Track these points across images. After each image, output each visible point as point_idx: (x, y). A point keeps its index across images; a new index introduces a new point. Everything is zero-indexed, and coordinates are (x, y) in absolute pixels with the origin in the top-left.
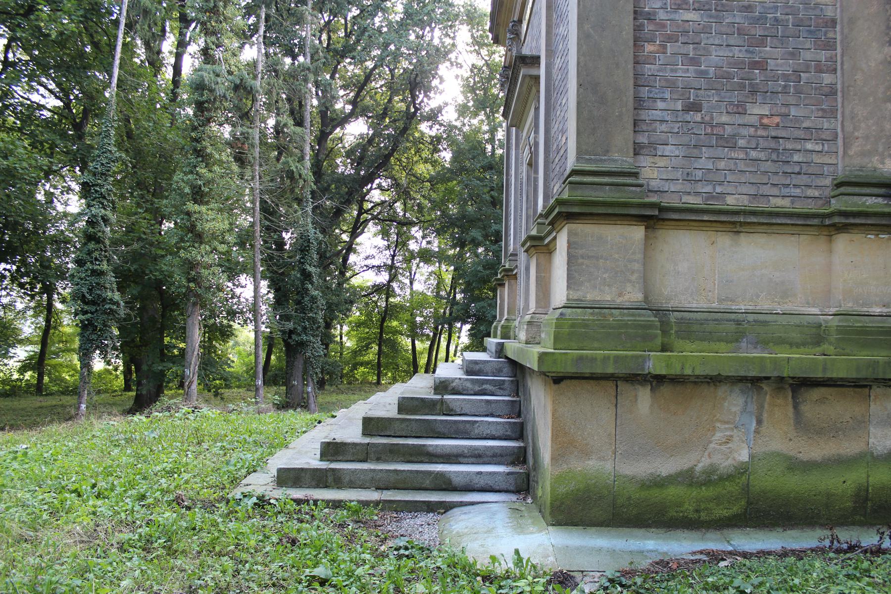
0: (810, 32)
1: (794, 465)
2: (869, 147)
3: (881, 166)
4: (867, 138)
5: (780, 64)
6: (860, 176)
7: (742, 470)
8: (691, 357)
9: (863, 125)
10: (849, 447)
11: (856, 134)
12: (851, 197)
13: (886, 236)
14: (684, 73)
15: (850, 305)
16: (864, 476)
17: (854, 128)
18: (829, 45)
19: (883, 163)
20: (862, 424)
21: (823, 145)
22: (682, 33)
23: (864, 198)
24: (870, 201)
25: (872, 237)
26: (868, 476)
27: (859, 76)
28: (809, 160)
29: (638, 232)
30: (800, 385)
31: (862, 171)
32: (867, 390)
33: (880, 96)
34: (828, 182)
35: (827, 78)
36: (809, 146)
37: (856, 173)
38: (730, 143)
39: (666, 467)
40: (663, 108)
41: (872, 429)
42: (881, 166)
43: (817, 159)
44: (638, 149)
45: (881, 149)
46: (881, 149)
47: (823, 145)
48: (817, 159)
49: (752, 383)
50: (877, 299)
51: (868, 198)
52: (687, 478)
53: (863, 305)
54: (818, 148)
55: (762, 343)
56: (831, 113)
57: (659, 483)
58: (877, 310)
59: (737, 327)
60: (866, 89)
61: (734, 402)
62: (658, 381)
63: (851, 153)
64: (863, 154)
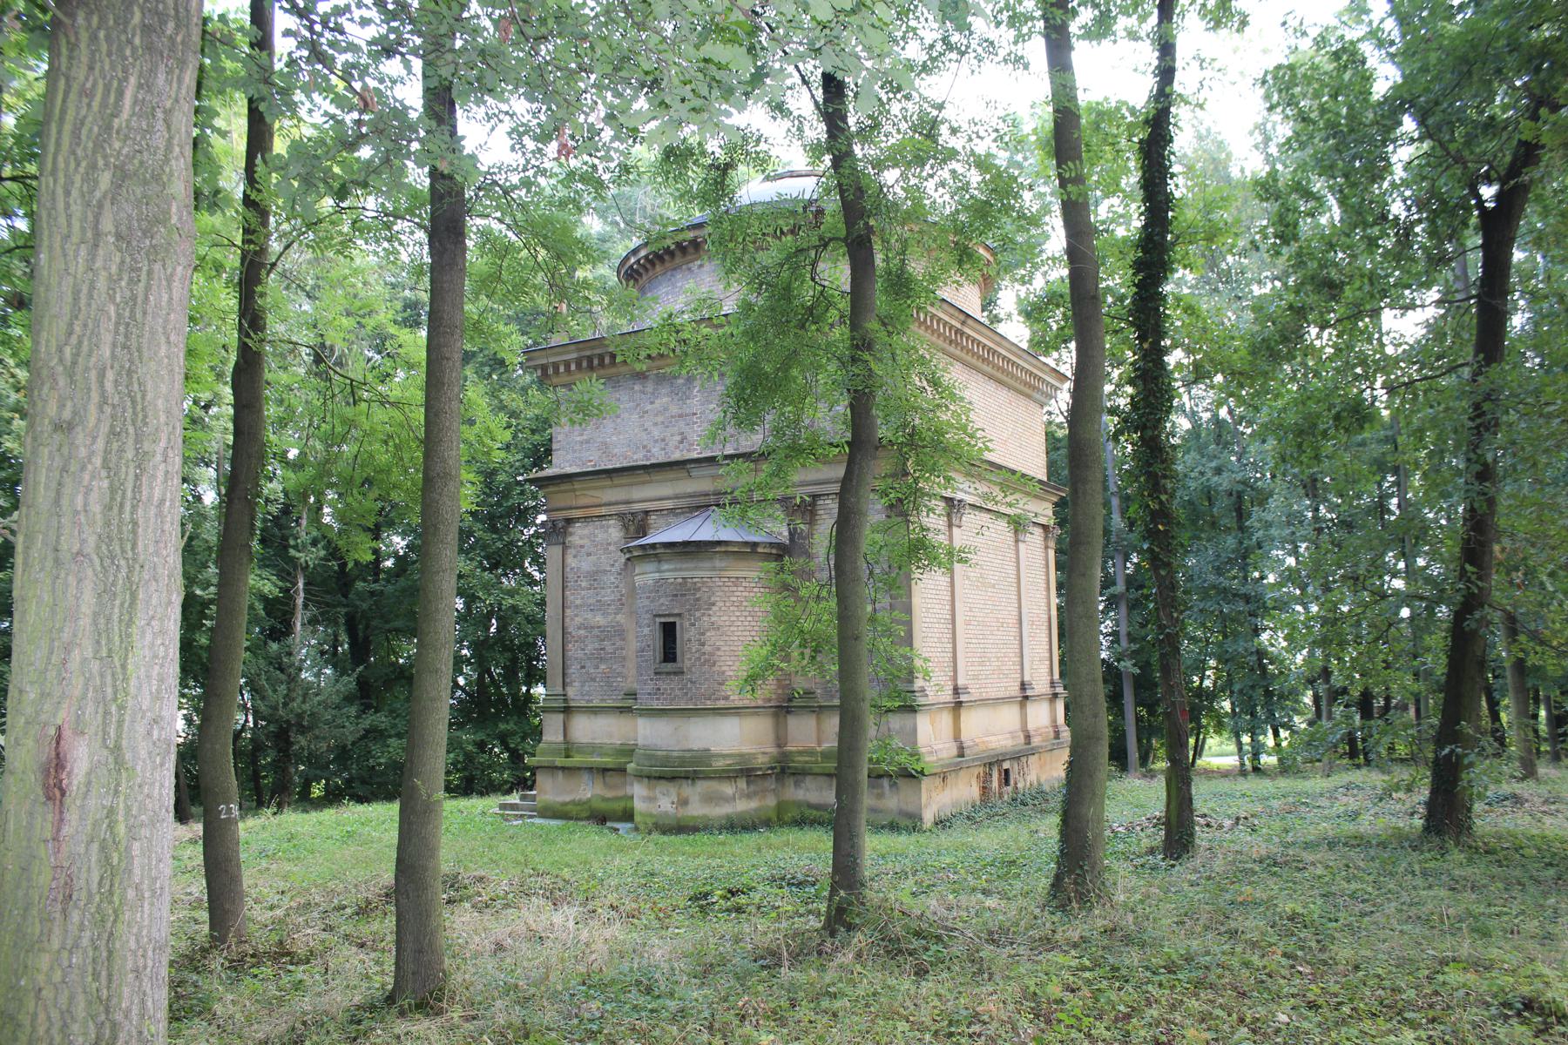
1: (604, 799)
5: (609, 649)
7: (589, 800)
8: (577, 760)
10: (620, 793)
14: (580, 654)
22: (581, 640)
29: (561, 716)
30: (604, 771)
38: (593, 680)
39: (568, 799)
40: (573, 669)
44: (564, 685)
49: (590, 769)
52: (573, 802)
55: (601, 755)
57: (566, 804)
59: (594, 749)
61: (586, 776)
62: (563, 768)
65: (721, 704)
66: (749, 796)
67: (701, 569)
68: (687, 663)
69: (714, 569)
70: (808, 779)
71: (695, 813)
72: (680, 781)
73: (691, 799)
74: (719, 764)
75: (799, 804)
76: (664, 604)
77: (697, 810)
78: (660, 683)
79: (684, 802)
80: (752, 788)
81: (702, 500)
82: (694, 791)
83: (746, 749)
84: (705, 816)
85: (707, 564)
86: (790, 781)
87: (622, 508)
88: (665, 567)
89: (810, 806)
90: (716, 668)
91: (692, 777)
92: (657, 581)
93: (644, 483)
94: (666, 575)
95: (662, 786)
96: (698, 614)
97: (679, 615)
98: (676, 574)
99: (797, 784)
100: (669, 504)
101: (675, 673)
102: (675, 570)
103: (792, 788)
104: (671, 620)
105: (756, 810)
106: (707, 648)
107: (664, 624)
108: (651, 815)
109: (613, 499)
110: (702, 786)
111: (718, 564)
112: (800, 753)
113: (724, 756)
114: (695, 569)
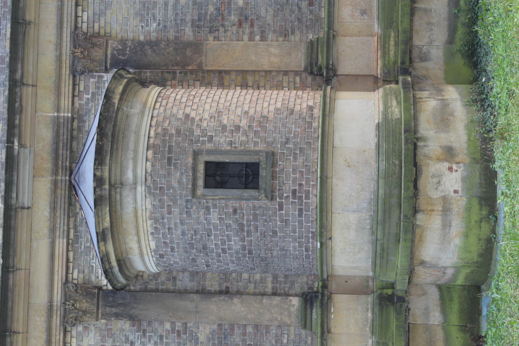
0: (225, 338)
2: (286, 313)
3: (296, 307)
4: (281, 314)
6: (301, 319)
9: (275, 315)
11: (279, 319)
12: (313, 326)
13: (332, 308)
15: (368, 329)
16: (454, 327)
17: (277, 320)
18: (232, 327)
19: (294, 305)
20: (428, 328)
21: (284, 334)
23: (313, 319)
24: (314, 316)
25: (333, 316)
26: (454, 325)
27: (249, 316)
28: (292, 341)
31: (298, 317)
32: (411, 326)
33: (259, 305)
34: (303, 332)
35: (249, 329)
36: (285, 341)
37: (300, 320)
41: (431, 323)
42: (296, 307)
43: (292, 337)
45: (286, 306)
46: (286, 306)
47: (284, 334)
48: (292, 337)
50: (364, 314)
51: (313, 317)
53: (367, 321)
54: (286, 336)
56: (267, 327)
58: (370, 315)
60: (256, 313)
63: (289, 322)
64: (290, 315)
65: (317, 112)
67: (139, 126)
68: (261, 147)
69: (143, 113)
70: (417, 41)
71: (464, 138)
72: (420, 157)
73: (445, 143)
74: (396, 111)
75: (449, 56)
76: (179, 179)
77: (459, 136)
78: (289, 186)
79: (449, 153)
81: (62, 192)
82: (433, 140)
84: (467, 127)
85: (135, 121)
86: (420, 67)
87: (56, 321)
88: (130, 175)
89: (451, 41)
90: (271, 116)
91: (413, 140)
92: (149, 191)
93: (29, 285)
94: (141, 173)
95: (427, 185)
96: (197, 132)
97: (196, 154)
98: (141, 157)
99: (424, 58)
100: (61, 244)
101: (274, 165)
102: (135, 160)
103: (429, 65)
104: (201, 168)
106: (244, 123)
107: (207, 186)
108: (468, 209)
109: (44, 336)
110: (426, 128)
111: (136, 110)
112: (385, 53)
113: (386, 107)
114: (137, 133)
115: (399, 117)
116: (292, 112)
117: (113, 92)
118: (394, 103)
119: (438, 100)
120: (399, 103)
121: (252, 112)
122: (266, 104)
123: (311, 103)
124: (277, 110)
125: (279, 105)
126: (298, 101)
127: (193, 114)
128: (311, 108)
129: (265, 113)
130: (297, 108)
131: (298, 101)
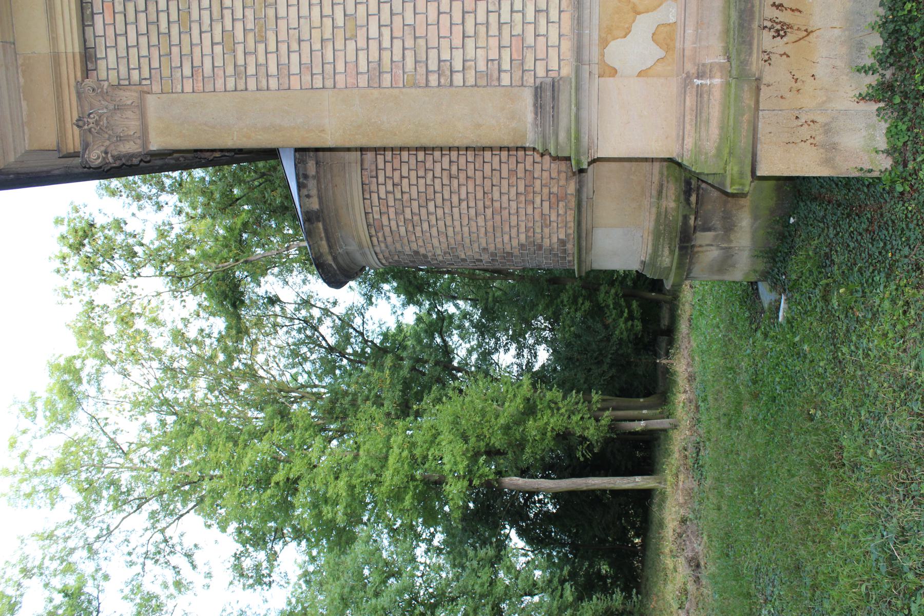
66: (729, 228)
80: (716, 222)
83: (649, 223)
105: (755, 218)
115: (669, 265)
116: (540, 247)
117: (321, 254)
118: (666, 252)
119: (722, 248)
120: (672, 252)
121: (492, 248)
122: (506, 238)
123: (562, 236)
124: (522, 246)
125: (523, 237)
126: (546, 230)
127: (422, 251)
128: (563, 243)
129: (508, 249)
130: (546, 242)
131: (546, 230)
